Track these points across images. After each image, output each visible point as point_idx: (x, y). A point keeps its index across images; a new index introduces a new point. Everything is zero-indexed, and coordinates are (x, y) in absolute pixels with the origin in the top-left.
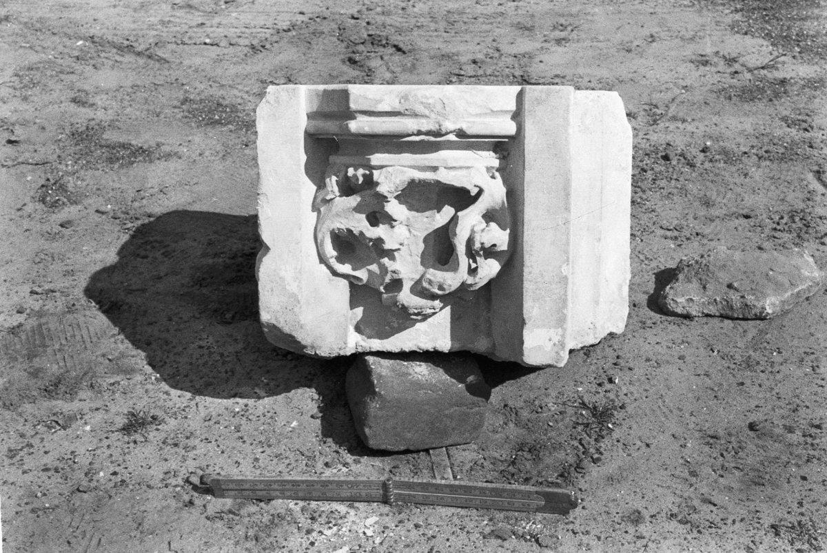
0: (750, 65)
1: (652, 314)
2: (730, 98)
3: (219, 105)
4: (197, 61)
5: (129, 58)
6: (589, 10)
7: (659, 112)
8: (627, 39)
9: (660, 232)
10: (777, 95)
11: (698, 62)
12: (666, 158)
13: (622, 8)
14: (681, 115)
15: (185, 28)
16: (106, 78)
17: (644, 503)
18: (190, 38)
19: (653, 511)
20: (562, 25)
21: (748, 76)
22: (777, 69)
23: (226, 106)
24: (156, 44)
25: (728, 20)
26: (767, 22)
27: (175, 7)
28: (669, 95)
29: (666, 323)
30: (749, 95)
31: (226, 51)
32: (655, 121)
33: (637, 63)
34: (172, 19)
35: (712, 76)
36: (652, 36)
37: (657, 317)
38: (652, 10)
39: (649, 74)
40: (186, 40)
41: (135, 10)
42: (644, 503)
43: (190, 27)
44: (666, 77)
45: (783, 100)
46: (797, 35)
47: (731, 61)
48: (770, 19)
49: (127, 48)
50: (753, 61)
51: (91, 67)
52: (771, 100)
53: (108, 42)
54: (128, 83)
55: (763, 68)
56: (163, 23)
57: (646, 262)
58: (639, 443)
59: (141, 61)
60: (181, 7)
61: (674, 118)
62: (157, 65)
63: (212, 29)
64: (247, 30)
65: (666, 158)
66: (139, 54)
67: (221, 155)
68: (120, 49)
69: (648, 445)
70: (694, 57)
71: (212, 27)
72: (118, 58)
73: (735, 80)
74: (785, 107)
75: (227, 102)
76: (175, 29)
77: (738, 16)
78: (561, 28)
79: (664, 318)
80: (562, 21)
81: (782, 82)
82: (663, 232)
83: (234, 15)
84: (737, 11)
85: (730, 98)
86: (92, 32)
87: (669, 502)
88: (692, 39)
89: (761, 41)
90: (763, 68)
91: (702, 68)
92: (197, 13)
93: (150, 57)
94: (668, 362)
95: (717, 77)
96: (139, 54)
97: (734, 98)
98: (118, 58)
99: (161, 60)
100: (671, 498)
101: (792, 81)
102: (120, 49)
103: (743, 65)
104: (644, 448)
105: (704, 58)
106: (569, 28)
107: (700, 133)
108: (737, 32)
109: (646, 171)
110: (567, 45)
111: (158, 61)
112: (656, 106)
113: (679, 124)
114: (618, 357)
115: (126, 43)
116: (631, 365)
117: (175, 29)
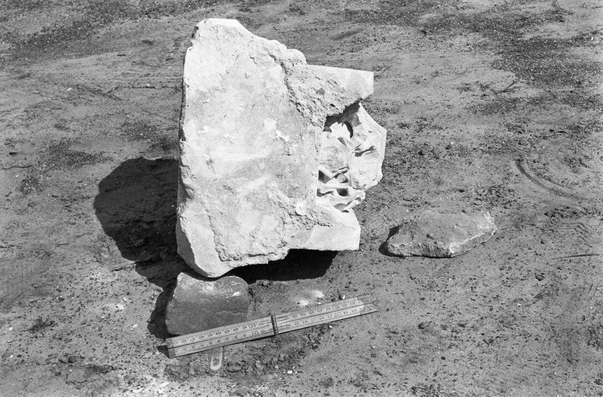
0: (496, 90)
1: (381, 255)
2: (475, 113)
6: (400, 56)
7: (425, 123)
8: (419, 75)
9: (402, 202)
10: (508, 110)
11: (463, 88)
12: (421, 153)
13: (422, 55)
14: (440, 125)
17: (336, 374)
19: (340, 378)
20: (379, 67)
21: (493, 97)
22: (514, 92)
25: (492, 60)
26: (517, 60)
27: (134, 64)
28: (437, 112)
29: (387, 261)
30: (489, 110)
31: (158, 91)
32: (421, 129)
33: (422, 92)
34: (130, 72)
35: (468, 99)
36: (437, 72)
37: (382, 256)
38: (442, 55)
39: (428, 99)
41: (109, 67)
42: (336, 374)
44: (438, 100)
45: (511, 113)
46: (535, 68)
47: (484, 87)
48: (520, 58)
50: (499, 87)
52: (503, 113)
55: (504, 91)
56: (123, 74)
57: (388, 222)
58: (345, 337)
60: (137, 64)
61: (435, 127)
63: (153, 78)
64: (176, 78)
65: (421, 153)
69: (351, 338)
70: (461, 86)
71: (154, 76)
73: (483, 101)
74: (511, 119)
77: (499, 57)
78: (378, 69)
79: (387, 257)
80: (381, 64)
81: (514, 100)
82: (404, 202)
83: (170, 68)
84: (499, 53)
85: (475, 113)
87: (352, 374)
88: (463, 73)
89: (510, 73)
90: (504, 91)
91: (464, 93)
92: (147, 67)
94: (380, 286)
95: (472, 98)
97: (478, 113)
100: (354, 371)
101: (521, 100)
103: (492, 90)
104: (348, 340)
105: (467, 86)
106: (383, 69)
107: (448, 136)
108: (495, 68)
109: (405, 163)
110: (379, 80)
112: (425, 120)
113: (437, 132)
114: (350, 283)
116: (356, 288)
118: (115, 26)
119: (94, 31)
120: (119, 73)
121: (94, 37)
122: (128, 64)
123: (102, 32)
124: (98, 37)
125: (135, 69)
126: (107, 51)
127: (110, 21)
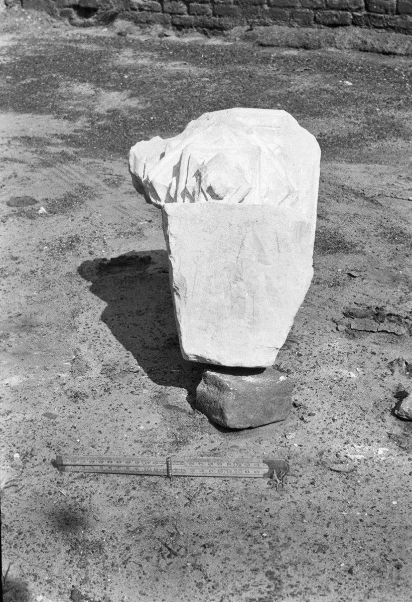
3: (401, 232)
4: (399, 207)
5: (360, 200)
15: (401, 189)
16: (342, 208)
18: (401, 195)
23: (404, 235)
24: (379, 195)
40: (398, 196)
41: (375, 176)
43: (404, 190)
49: (360, 194)
51: (336, 201)
53: (351, 190)
54: (354, 212)
56: (388, 184)
59: (366, 203)
62: (374, 206)
66: (367, 199)
67: (390, 258)
68: (357, 194)
72: (353, 199)
75: (407, 232)
76: (395, 189)
86: (346, 183)
93: (372, 201)
96: (367, 199)
98: (353, 199)
99: (377, 204)
102: (357, 194)
111: (376, 204)
115: (361, 192)
117: (395, 189)
118: (387, 143)
119: (367, 143)
120: (384, 183)
121: (366, 149)
122: (394, 178)
123: (374, 146)
124: (370, 150)
125: (400, 182)
126: (376, 162)
127: (384, 138)
